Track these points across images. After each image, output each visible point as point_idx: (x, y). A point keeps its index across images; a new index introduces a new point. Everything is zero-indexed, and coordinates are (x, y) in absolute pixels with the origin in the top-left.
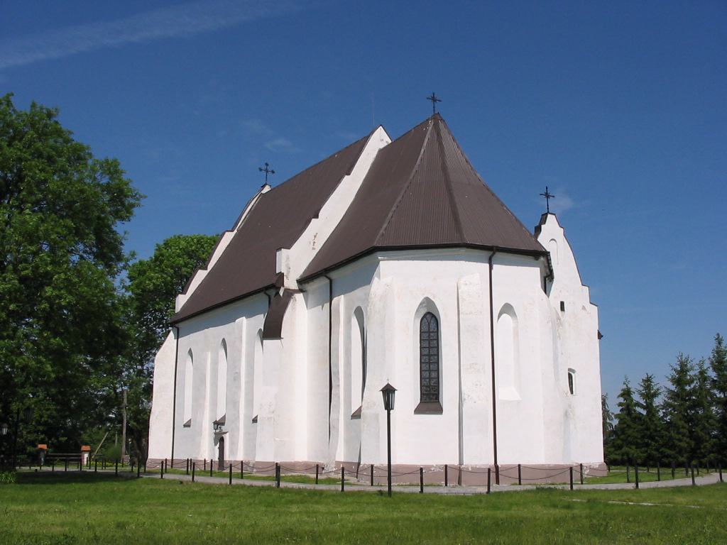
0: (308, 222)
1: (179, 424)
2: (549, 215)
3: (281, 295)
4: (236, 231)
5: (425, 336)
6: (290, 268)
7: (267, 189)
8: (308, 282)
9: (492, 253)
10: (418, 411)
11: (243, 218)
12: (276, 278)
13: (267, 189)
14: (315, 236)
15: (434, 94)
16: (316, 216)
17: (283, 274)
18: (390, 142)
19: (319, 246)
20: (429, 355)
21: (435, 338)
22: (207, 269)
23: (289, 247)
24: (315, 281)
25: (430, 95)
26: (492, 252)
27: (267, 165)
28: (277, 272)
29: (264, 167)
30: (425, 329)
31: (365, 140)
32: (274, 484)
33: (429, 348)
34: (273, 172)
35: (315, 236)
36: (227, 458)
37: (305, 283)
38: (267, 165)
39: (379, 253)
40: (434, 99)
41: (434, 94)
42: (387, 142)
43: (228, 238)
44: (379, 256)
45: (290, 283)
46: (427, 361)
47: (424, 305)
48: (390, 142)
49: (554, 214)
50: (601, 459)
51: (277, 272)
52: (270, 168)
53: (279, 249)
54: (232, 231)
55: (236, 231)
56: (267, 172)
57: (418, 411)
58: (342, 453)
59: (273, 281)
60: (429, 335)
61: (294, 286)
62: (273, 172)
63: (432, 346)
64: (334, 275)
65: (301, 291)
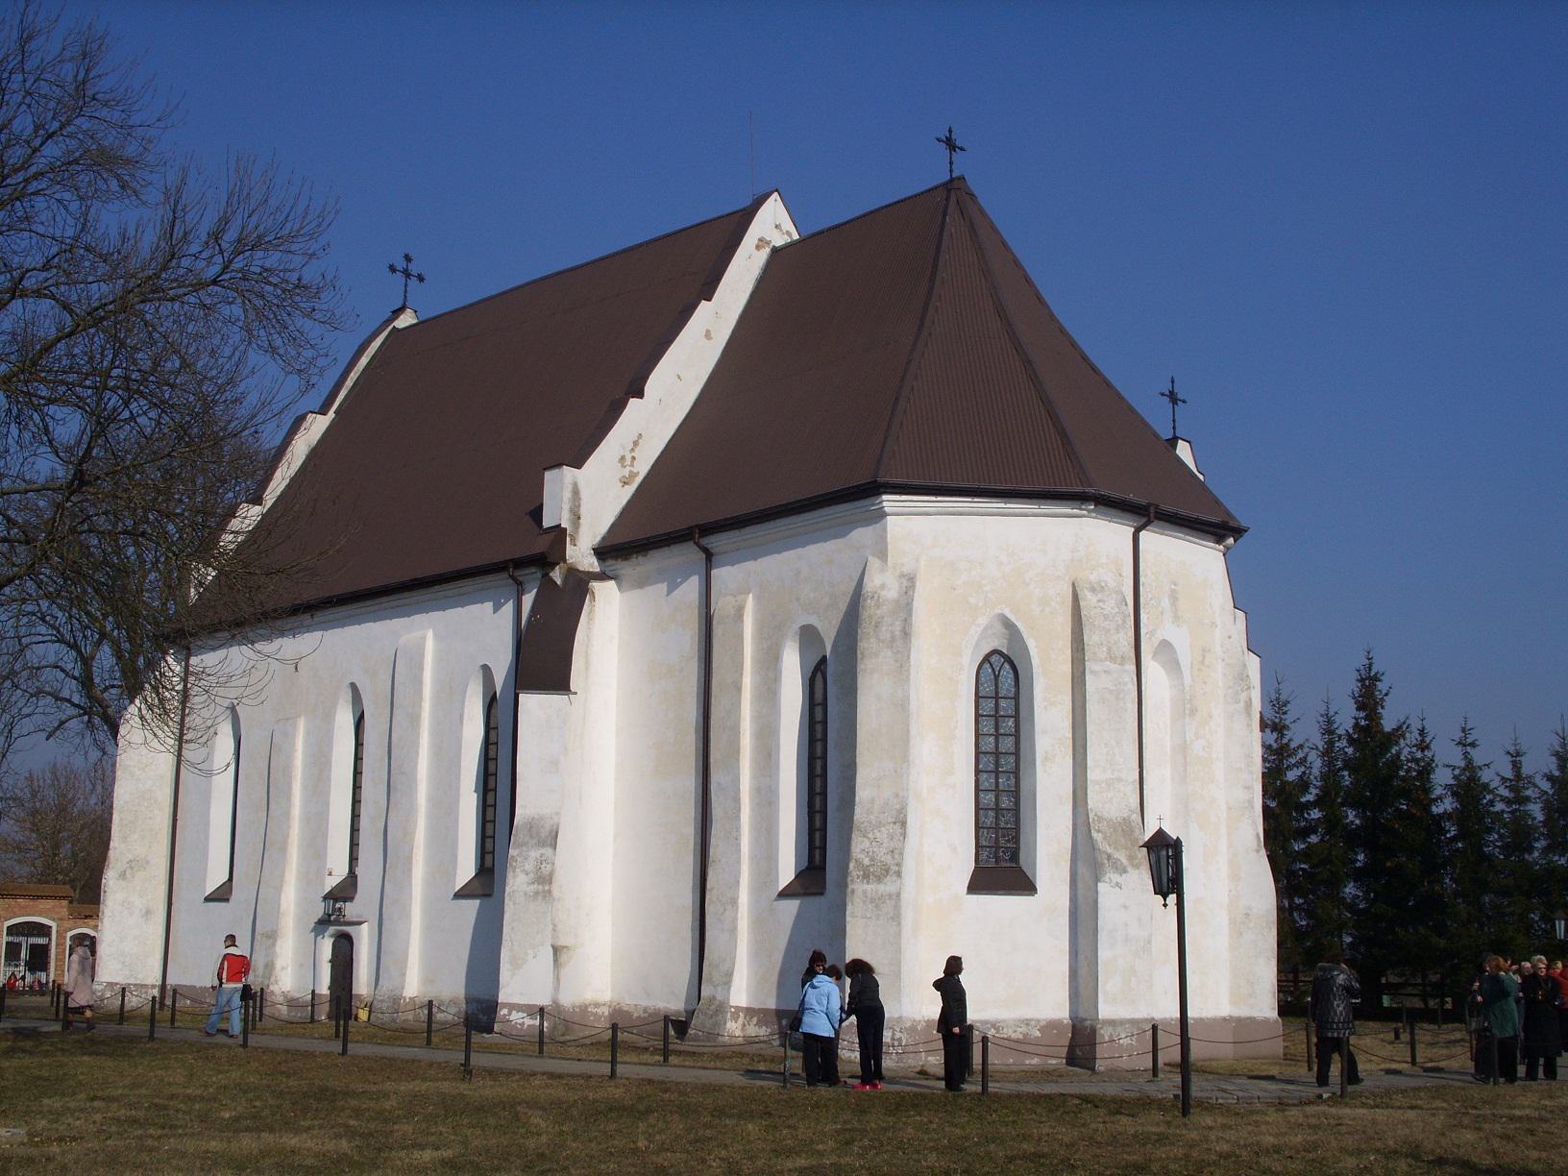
0: (616, 409)
1: (189, 899)
2: (1180, 441)
3: (559, 582)
4: (331, 414)
5: (988, 706)
6: (579, 518)
7: (406, 320)
8: (625, 558)
9: (1144, 520)
10: (977, 885)
11: (349, 383)
12: (548, 538)
13: (406, 320)
14: (636, 443)
15: (950, 131)
16: (640, 394)
17: (566, 529)
18: (796, 237)
19: (643, 468)
20: (997, 754)
21: (1011, 712)
22: (257, 500)
23: (579, 466)
24: (634, 560)
25: (943, 134)
26: (1144, 513)
27: (408, 258)
28: (547, 523)
29: (401, 264)
30: (988, 689)
31: (745, 217)
32: (336, 1047)
33: (997, 736)
34: (421, 278)
35: (636, 443)
36: (362, 983)
37: (616, 558)
38: (408, 258)
39: (885, 497)
40: (950, 144)
41: (950, 131)
42: (788, 233)
43: (317, 427)
44: (889, 501)
45: (581, 554)
46: (992, 767)
47: (990, 632)
48: (796, 237)
49: (1189, 442)
50: (1264, 1004)
51: (547, 523)
52: (414, 269)
53: (559, 465)
54: (323, 411)
55: (331, 414)
56: (407, 274)
57: (977, 885)
58: (744, 985)
59: (540, 545)
60: (997, 705)
61: (589, 563)
62: (421, 278)
63: (1002, 731)
64: (714, 542)
65: (602, 576)
